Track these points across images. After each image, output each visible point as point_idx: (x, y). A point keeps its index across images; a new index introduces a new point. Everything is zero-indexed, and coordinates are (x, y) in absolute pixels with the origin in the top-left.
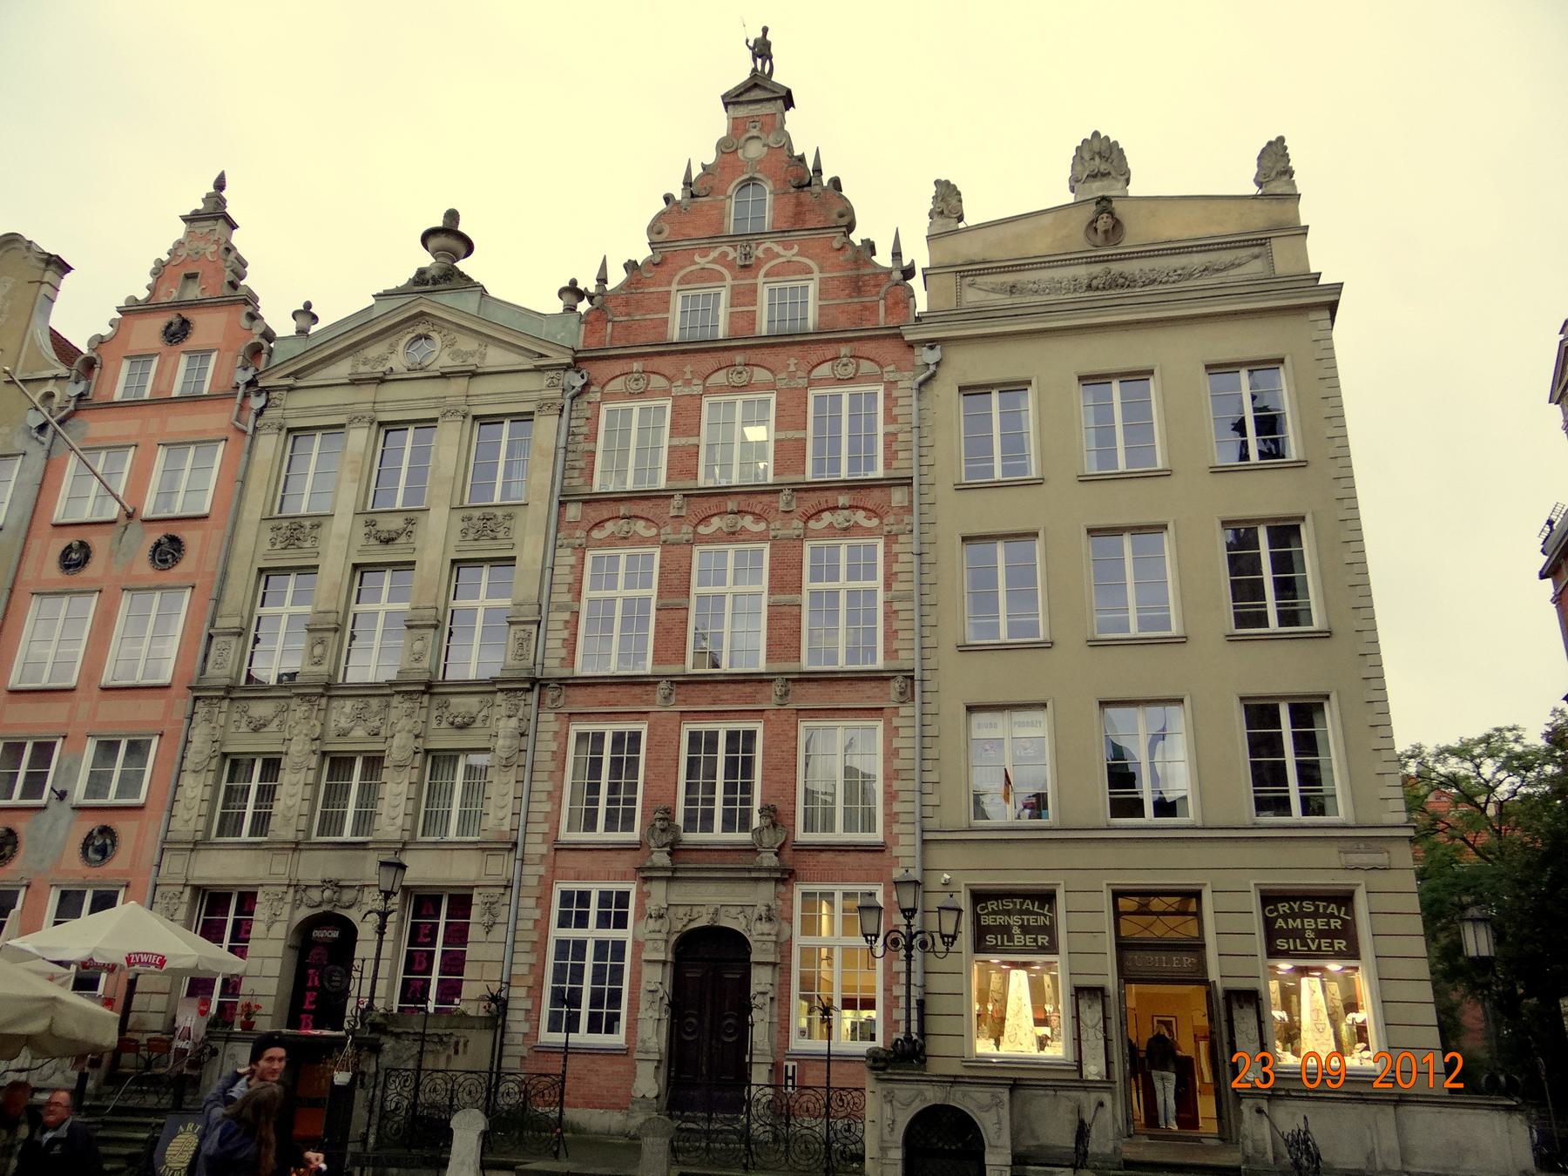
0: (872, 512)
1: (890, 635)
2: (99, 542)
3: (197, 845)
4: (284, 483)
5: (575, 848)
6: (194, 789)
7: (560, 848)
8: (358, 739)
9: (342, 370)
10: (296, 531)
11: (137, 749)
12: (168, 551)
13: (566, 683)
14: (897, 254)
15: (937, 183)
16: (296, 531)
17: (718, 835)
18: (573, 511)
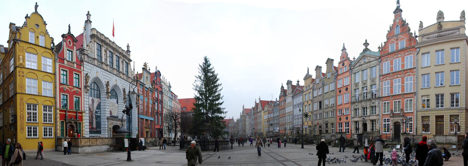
0: (412, 72)
1: (414, 88)
2: (341, 89)
3: (354, 118)
4: (355, 79)
5: (384, 115)
6: (353, 112)
7: (383, 115)
8: (365, 106)
9: (358, 65)
10: (357, 85)
11: (348, 109)
12: (347, 89)
13: (382, 97)
14: (415, 34)
15: (421, 21)
16: (357, 85)
17: (397, 112)
18: (381, 77)
